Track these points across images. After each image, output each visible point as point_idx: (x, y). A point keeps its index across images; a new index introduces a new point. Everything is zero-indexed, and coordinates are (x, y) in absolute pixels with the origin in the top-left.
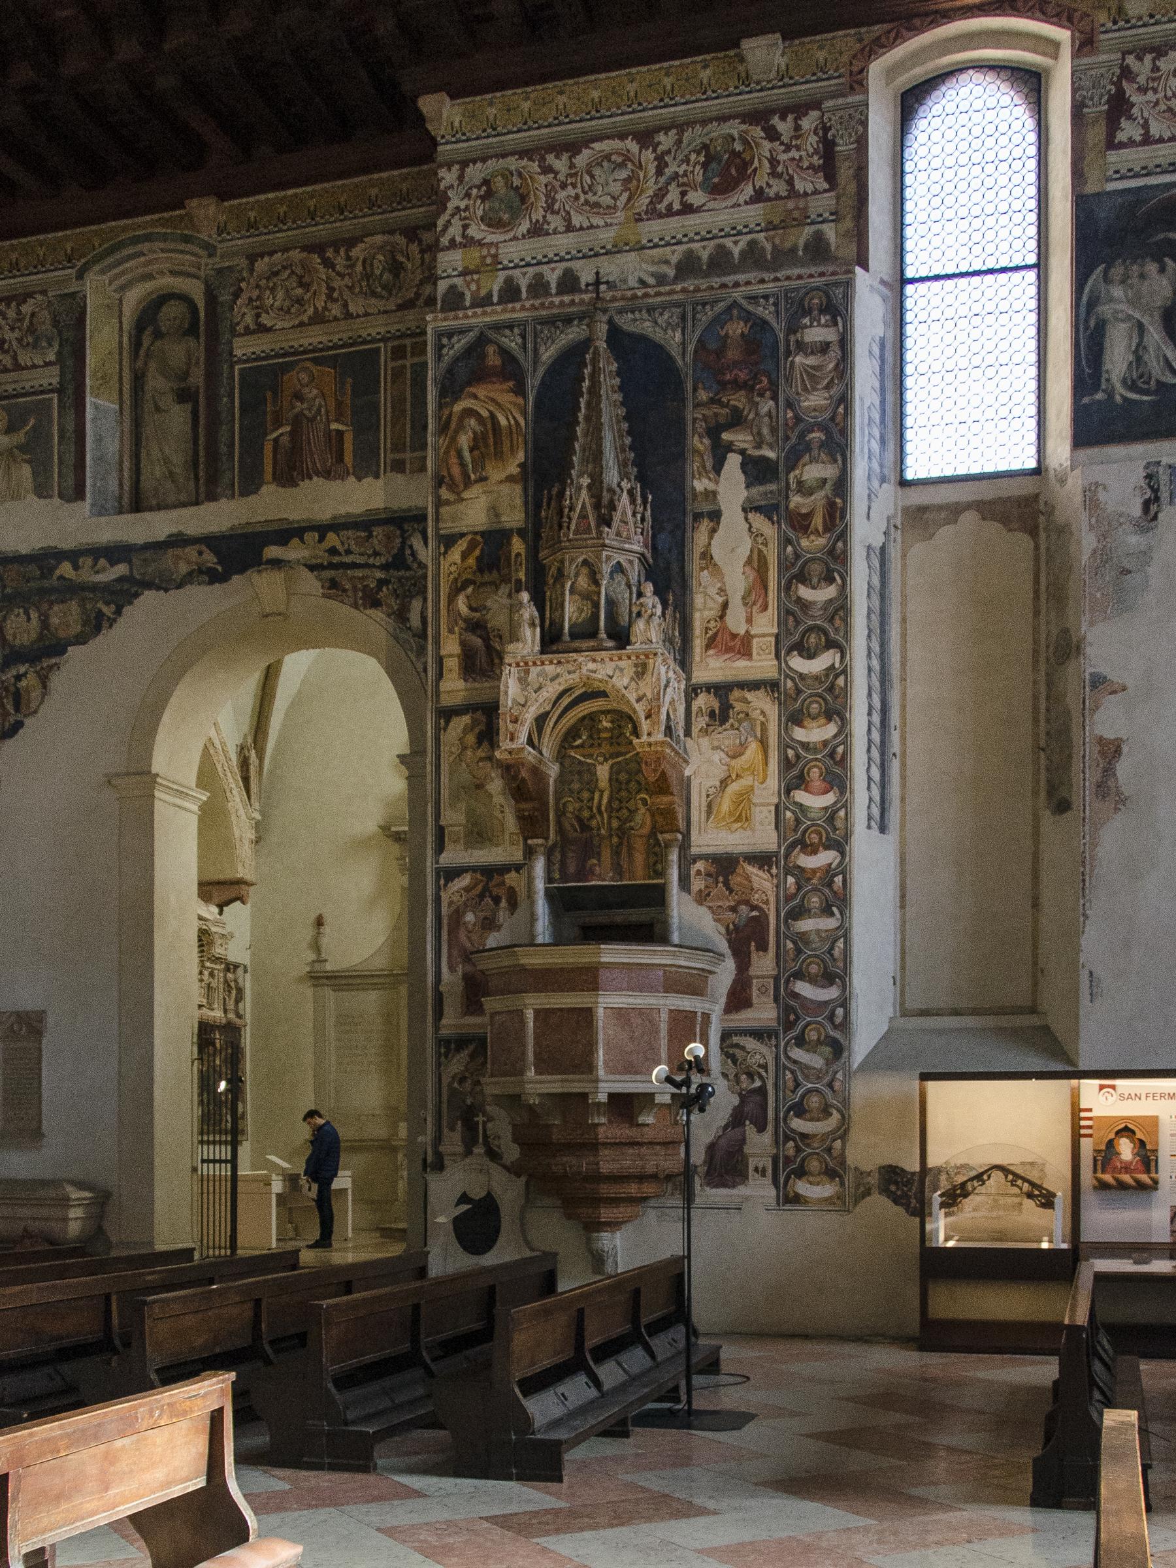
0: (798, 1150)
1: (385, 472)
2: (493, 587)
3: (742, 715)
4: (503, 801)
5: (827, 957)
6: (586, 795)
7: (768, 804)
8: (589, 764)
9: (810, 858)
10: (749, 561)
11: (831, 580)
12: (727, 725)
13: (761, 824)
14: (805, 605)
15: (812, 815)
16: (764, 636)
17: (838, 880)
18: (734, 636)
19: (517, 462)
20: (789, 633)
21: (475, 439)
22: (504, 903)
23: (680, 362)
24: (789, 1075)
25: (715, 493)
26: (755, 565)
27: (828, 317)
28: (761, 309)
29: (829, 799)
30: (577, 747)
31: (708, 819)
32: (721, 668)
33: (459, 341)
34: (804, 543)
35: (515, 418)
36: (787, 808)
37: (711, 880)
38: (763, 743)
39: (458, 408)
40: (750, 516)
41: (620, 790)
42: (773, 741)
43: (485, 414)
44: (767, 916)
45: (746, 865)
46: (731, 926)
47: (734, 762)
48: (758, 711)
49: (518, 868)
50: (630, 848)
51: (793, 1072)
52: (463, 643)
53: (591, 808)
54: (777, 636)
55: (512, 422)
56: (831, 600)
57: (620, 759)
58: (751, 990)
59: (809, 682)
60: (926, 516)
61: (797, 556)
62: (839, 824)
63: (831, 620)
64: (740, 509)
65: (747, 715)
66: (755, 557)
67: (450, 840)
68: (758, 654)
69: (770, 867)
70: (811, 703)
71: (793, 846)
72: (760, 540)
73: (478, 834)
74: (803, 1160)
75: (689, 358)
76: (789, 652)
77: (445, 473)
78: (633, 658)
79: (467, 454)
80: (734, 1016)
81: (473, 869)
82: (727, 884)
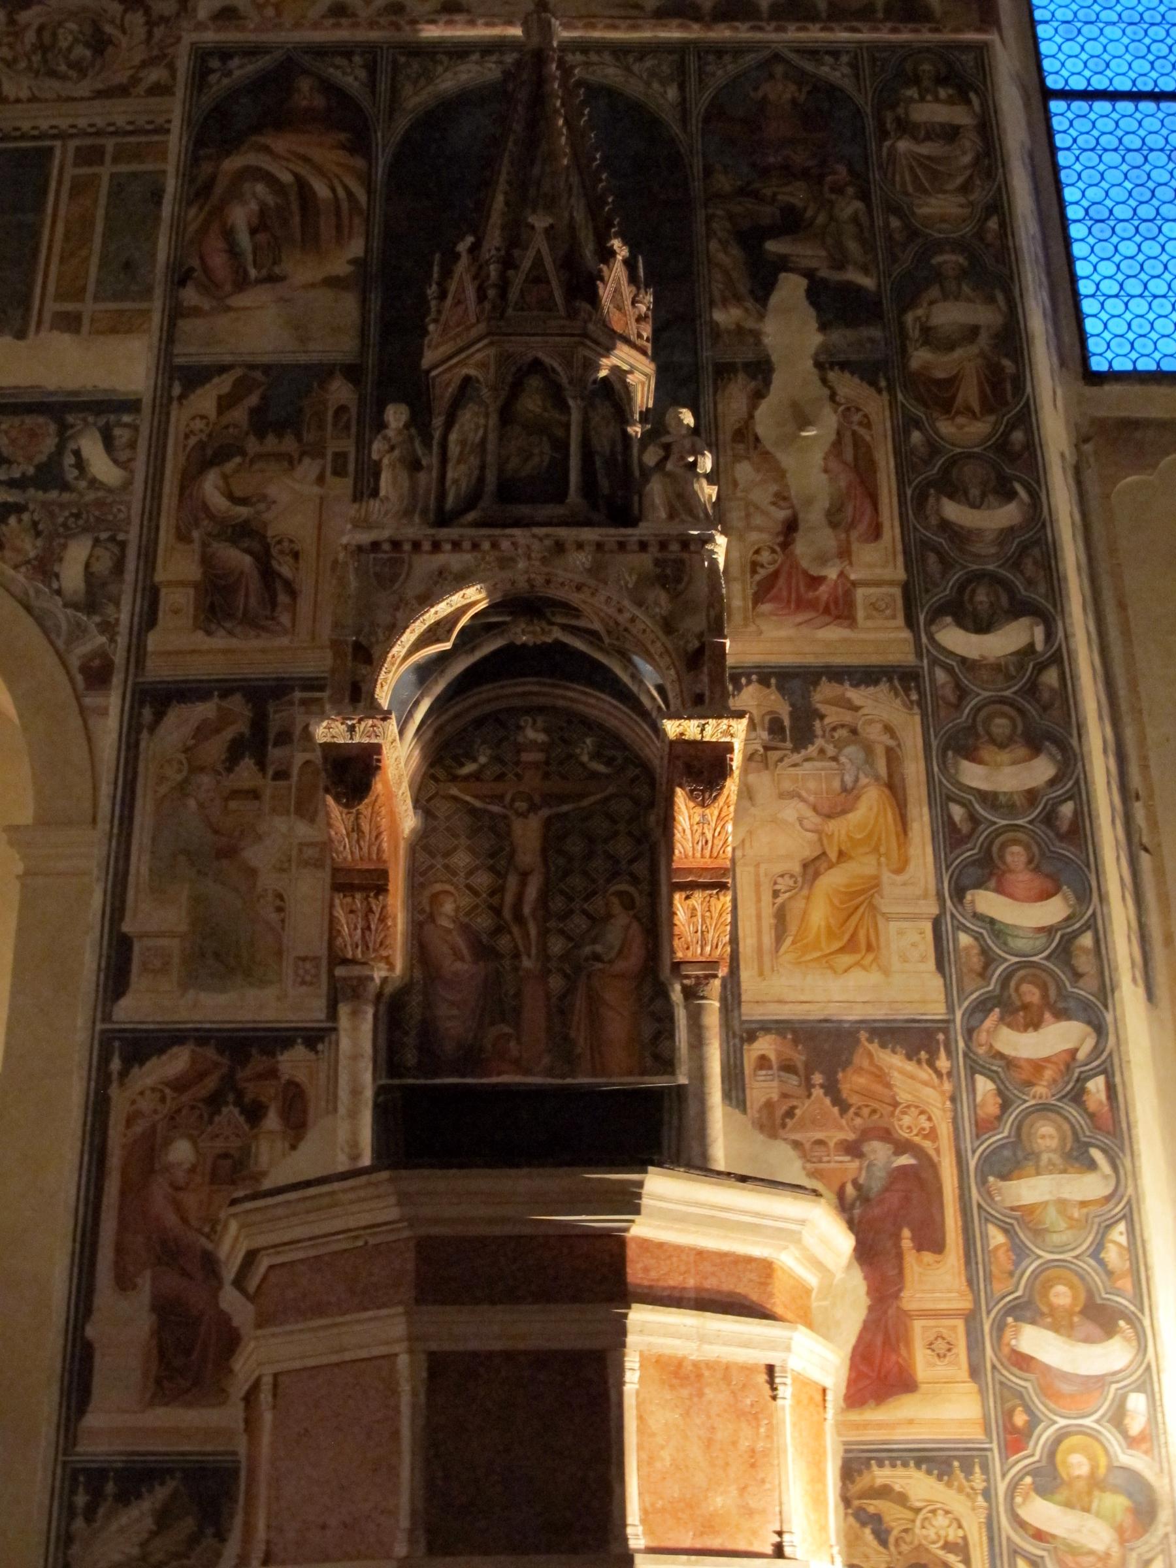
1: (39, 324)
5: (1088, 1266)
8: (492, 816)
12: (812, 750)
14: (958, 535)
15: (1019, 944)
17: (1097, 1085)
19: (351, 256)
21: (263, 212)
23: (676, 129)
25: (757, 335)
27: (950, 91)
28: (826, 69)
29: (1053, 911)
30: (467, 778)
31: (779, 939)
32: (790, 639)
33: (241, 67)
34: (946, 428)
35: (346, 188)
37: (794, 1080)
38: (894, 788)
39: (233, 163)
40: (832, 376)
41: (567, 873)
43: (286, 178)
44: (934, 1167)
45: (874, 1047)
46: (850, 1190)
47: (832, 826)
48: (879, 726)
50: (594, 1000)
52: (206, 561)
53: (497, 911)
55: (341, 193)
57: (565, 808)
58: (908, 1344)
60: (1138, 435)
61: (934, 449)
62: (1084, 963)
64: (810, 362)
65: (854, 732)
67: (145, 968)
68: (868, 617)
71: (982, 1007)
72: (856, 418)
75: (695, 124)
76: (931, 621)
77: (195, 263)
78: (654, 550)
79: (244, 240)
80: (874, 1415)
82: (832, 1089)
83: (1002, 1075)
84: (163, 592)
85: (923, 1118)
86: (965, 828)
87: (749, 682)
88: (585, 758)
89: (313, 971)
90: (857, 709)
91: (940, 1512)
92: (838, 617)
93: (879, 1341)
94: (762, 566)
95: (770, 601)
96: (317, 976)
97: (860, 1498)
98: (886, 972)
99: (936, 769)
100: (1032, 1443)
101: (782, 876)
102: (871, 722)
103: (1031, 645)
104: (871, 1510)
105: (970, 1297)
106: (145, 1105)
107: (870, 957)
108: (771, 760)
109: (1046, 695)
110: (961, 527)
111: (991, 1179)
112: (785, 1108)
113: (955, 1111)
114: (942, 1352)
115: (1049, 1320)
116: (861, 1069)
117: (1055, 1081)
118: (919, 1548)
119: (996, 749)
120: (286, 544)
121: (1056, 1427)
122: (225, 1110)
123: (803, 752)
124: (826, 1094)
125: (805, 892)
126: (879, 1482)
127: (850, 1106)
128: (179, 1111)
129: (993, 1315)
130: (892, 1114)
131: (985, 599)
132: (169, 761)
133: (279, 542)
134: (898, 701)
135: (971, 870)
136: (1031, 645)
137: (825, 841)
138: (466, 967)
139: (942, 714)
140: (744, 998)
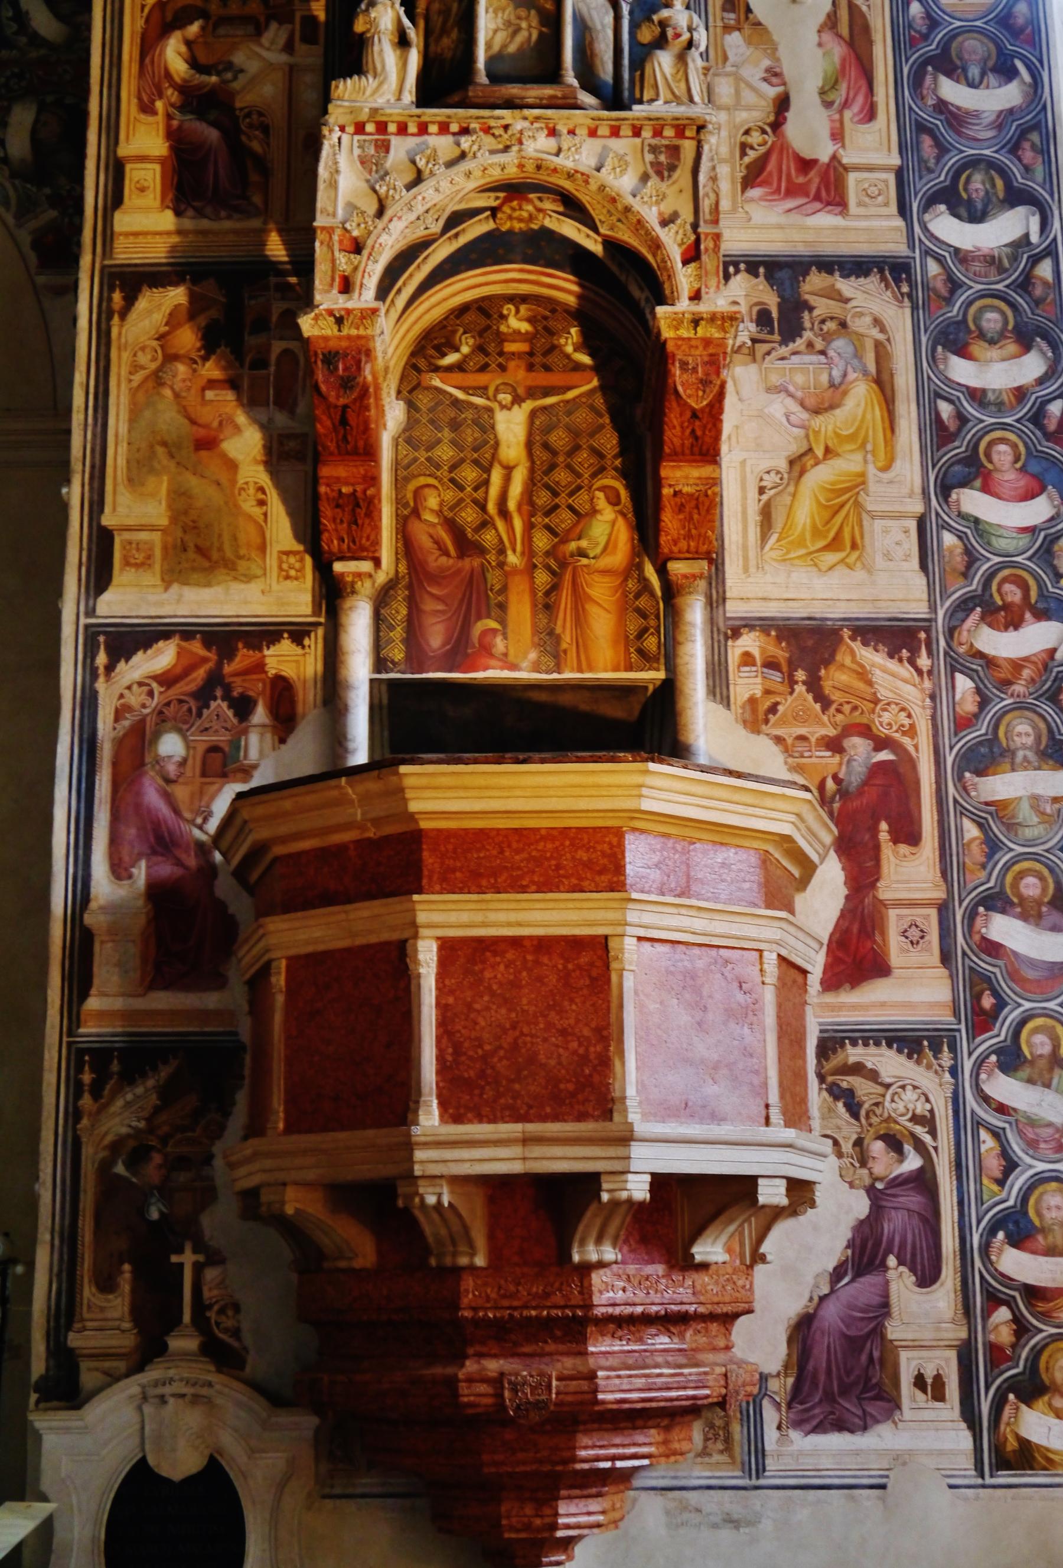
0: (1021, 1329)
2: (251, 29)
3: (831, 326)
4: (264, 478)
6: (469, 474)
7: (900, 516)
9: (1011, 635)
10: (831, 22)
11: (1008, 73)
12: (800, 343)
13: (888, 556)
15: (1001, 544)
16: (870, 169)
18: (806, 165)
20: (925, 168)
22: (260, 715)
24: (988, 1142)
26: (844, 30)
30: (449, 369)
31: (764, 538)
32: (780, 227)
36: (946, 526)
37: (776, 676)
41: (552, 467)
42: (904, 381)
44: (912, 764)
45: (857, 646)
46: (830, 785)
47: (818, 422)
48: (868, 320)
49: (298, 634)
50: (580, 599)
51: (997, 1134)
52: (174, 136)
53: (483, 507)
54: (900, 174)
56: (1011, 111)
58: (883, 933)
59: (977, 267)
61: (933, 23)
63: (1014, 149)
65: (843, 325)
66: (844, 14)
69: (914, 653)
70: (982, 310)
73: (199, 550)
74: (1037, 1353)
80: (848, 997)
81: (185, 632)
82: (814, 686)
83: (982, 674)
84: (128, 167)
85: (903, 714)
86: (952, 426)
87: (737, 271)
88: (569, 349)
89: (298, 565)
90: (847, 301)
91: (909, 1087)
92: (828, 204)
93: (855, 929)
94: (752, 148)
95: (759, 185)
96: (301, 570)
97: (833, 1074)
98: (869, 570)
99: (925, 364)
100: (998, 1025)
101: (768, 472)
102: (861, 315)
103: (1027, 236)
104: (844, 1085)
105: (944, 888)
106: (135, 699)
107: (855, 555)
108: (759, 355)
109: (1038, 291)
110: (958, 108)
111: (967, 775)
112: (767, 704)
113: (935, 708)
114: (915, 939)
115: (1019, 910)
116: (843, 665)
117: (1033, 681)
118: (889, 1119)
119: (986, 345)
120: (255, 117)
121: (1021, 1009)
122: (213, 705)
123: (791, 346)
124: (808, 691)
125: (791, 489)
126: (852, 1060)
127: (832, 702)
128: (168, 704)
129: (965, 904)
130: (873, 711)
131: (980, 186)
132: (143, 349)
133: (248, 115)
134: (889, 293)
135: (957, 468)
136: (1027, 236)
137: (812, 438)
138: (451, 561)
139: (933, 305)
140: (728, 595)
